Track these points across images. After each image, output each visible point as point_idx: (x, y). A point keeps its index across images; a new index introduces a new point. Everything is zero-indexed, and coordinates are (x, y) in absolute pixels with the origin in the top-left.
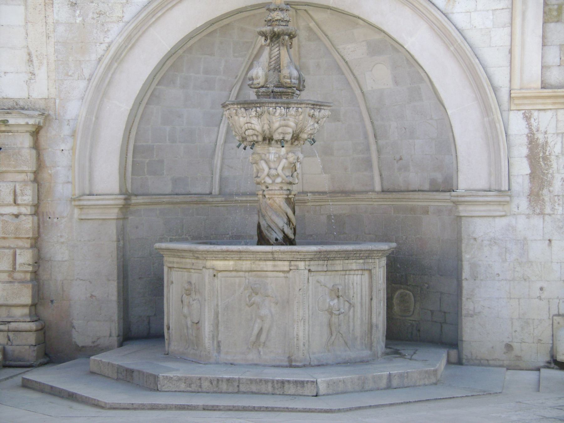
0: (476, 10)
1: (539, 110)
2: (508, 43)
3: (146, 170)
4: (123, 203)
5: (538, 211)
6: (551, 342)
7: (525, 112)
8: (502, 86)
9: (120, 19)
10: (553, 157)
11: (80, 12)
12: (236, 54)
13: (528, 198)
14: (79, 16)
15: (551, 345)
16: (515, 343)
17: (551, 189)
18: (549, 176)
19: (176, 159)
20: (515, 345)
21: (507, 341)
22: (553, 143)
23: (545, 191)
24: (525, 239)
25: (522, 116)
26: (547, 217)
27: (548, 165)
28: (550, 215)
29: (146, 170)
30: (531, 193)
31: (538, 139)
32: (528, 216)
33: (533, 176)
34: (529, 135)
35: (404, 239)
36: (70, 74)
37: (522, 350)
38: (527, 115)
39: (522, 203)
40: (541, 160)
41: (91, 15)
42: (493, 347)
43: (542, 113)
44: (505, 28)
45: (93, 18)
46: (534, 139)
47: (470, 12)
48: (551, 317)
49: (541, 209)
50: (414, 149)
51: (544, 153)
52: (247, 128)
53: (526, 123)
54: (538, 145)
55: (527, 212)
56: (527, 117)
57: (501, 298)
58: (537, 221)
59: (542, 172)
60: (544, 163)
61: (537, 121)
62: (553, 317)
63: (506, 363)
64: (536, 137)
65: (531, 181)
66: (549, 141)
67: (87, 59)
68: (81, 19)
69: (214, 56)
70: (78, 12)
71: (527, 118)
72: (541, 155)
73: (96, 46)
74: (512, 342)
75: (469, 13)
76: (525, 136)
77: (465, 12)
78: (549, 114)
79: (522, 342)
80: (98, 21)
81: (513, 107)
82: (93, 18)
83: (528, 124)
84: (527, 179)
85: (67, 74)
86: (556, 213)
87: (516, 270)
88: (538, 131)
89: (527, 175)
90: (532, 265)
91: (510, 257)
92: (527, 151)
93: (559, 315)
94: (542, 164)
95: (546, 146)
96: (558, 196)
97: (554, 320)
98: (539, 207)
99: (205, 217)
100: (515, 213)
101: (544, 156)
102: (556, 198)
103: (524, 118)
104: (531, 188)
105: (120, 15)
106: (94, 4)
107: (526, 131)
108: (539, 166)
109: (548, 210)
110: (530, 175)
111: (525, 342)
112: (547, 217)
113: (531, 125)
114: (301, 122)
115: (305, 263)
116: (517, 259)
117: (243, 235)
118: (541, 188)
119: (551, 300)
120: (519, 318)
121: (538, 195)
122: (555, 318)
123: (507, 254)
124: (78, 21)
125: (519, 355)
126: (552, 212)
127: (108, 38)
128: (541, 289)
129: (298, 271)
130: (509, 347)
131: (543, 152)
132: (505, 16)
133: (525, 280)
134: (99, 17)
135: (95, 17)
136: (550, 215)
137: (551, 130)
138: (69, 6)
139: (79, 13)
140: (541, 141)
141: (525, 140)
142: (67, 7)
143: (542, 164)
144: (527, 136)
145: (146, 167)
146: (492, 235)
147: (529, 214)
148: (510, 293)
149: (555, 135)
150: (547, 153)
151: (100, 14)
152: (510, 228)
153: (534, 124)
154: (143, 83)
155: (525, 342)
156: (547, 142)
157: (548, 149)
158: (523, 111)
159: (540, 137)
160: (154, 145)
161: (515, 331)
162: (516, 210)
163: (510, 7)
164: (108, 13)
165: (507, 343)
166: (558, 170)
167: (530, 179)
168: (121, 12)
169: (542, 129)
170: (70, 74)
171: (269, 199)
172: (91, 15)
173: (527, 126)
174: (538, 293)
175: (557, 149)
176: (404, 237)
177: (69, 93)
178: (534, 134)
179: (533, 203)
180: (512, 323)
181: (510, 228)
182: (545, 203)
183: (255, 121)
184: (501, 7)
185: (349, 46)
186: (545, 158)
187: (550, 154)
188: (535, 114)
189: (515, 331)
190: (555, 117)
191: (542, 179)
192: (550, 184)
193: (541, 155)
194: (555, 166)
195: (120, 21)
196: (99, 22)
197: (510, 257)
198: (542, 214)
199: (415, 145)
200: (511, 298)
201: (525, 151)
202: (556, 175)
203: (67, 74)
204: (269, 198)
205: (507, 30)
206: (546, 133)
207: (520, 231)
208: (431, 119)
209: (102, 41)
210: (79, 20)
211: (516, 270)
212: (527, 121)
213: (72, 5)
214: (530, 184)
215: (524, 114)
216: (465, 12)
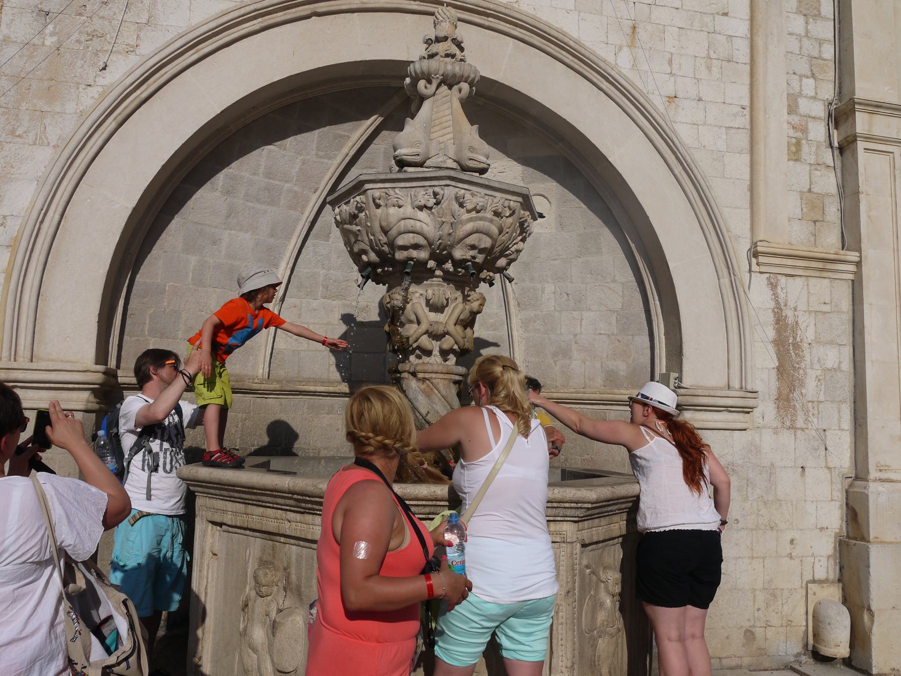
0: (705, 124)
1: (787, 275)
2: (747, 176)
3: (147, 327)
4: (100, 381)
5: (788, 423)
6: (804, 624)
7: (770, 276)
8: (741, 236)
9: (132, 49)
10: (805, 346)
11: (55, 28)
12: (321, 153)
13: (775, 403)
14: (52, 34)
15: (804, 628)
16: (758, 629)
17: (804, 391)
18: (801, 372)
19: (202, 313)
20: (759, 632)
21: (747, 625)
22: (805, 324)
23: (796, 395)
24: (772, 465)
25: (766, 282)
26: (799, 432)
27: (799, 356)
28: (803, 430)
29: (147, 327)
30: (779, 397)
31: (786, 316)
32: (776, 431)
33: (781, 370)
34: (776, 310)
35: (562, 461)
36: (17, 133)
37: (766, 639)
38: (772, 280)
39: (766, 410)
40: (791, 348)
41: (75, 36)
42: (728, 638)
43: (790, 279)
44: (742, 155)
45: (78, 41)
46: (782, 316)
47: (698, 125)
48: (804, 585)
49: (792, 420)
50: (581, 325)
51: (795, 338)
52: (402, 229)
53: (772, 292)
54: (787, 325)
55: (775, 425)
56: (772, 284)
57: (740, 557)
58: (786, 437)
59: (793, 366)
60: (795, 352)
61: (784, 291)
62: (807, 585)
63: (746, 661)
64: (784, 315)
65: (778, 378)
66: (800, 322)
67: (58, 109)
68: (55, 39)
69: (285, 149)
70: (50, 27)
71: (773, 286)
72: (791, 341)
73: (78, 88)
74: (754, 626)
75: (696, 126)
76: (770, 311)
77: (690, 124)
78: (799, 282)
79: (767, 626)
80: (88, 47)
81: (755, 268)
82: (78, 41)
83: (774, 294)
84: (774, 373)
85: (13, 132)
86: (810, 427)
87: (761, 513)
88: (786, 305)
89: (774, 368)
90: (781, 505)
91: (753, 493)
92: (774, 334)
93: (814, 581)
94: (793, 354)
95: (797, 328)
96: (813, 402)
97: (809, 589)
98: (789, 417)
99: (244, 415)
100: (760, 425)
101: (794, 342)
102: (810, 404)
103: (768, 285)
104: (779, 389)
105: (133, 42)
106: (83, 18)
107: (772, 304)
108: (789, 357)
109: (800, 423)
110: (778, 368)
111: (771, 626)
112: (799, 432)
113: (778, 297)
114: (508, 230)
115: (578, 525)
116: (762, 497)
117: (304, 447)
118: (792, 389)
119: (804, 559)
120: (764, 589)
121: (788, 400)
122: (809, 585)
123: (749, 489)
124: (48, 43)
125: (763, 647)
126: (805, 426)
127: (103, 78)
128: (792, 542)
129: (564, 545)
130: (749, 635)
131: (793, 337)
132: (743, 140)
133: (772, 528)
134: (91, 40)
135: (83, 39)
136: (803, 430)
137: (802, 307)
138: (35, 14)
139: (52, 30)
140: (790, 320)
141: (771, 318)
142: (29, 15)
143: (793, 354)
144: (773, 311)
145: (147, 322)
146: (729, 458)
147: (777, 428)
148: (752, 549)
149: (807, 313)
150: (798, 339)
151: (92, 36)
152: (753, 449)
153: (782, 295)
154: (163, 163)
155: (771, 626)
156: (797, 322)
157: (799, 332)
158: (768, 275)
159: (789, 313)
160: (166, 285)
161: (758, 610)
162: (760, 420)
163: (748, 127)
164: (108, 36)
165: (747, 628)
166: (812, 364)
167: (778, 375)
168: (135, 37)
169: (791, 304)
170: (17, 133)
171: (424, 380)
172: (75, 36)
173: (773, 297)
174: (788, 549)
175: (810, 335)
176: (563, 457)
177: (12, 167)
178: (781, 310)
179: (782, 410)
180: (755, 597)
181: (753, 449)
182: (797, 412)
183: (423, 215)
184: (737, 126)
185: (496, 164)
186: (797, 346)
187: (801, 341)
188: (783, 280)
189: (758, 610)
190: (805, 287)
191: (793, 376)
192: (802, 384)
193: (791, 341)
194: (808, 358)
195: (131, 51)
196: (90, 48)
197: (753, 493)
198: (793, 427)
199: (582, 319)
200: (753, 558)
201: (771, 333)
202: (809, 371)
203: (13, 132)
204: (424, 378)
205: (746, 158)
206: (795, 309)
207: (766, 453)
208: (614, 281)
209: (91, 82)
210: (50, 41)
211: (761, 513)
212: (772, 290)
213: (38, 15)
214: (777, 383)
215: (768, 279)
216: (690, 124)
